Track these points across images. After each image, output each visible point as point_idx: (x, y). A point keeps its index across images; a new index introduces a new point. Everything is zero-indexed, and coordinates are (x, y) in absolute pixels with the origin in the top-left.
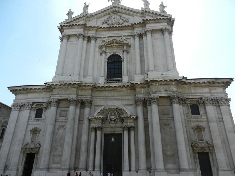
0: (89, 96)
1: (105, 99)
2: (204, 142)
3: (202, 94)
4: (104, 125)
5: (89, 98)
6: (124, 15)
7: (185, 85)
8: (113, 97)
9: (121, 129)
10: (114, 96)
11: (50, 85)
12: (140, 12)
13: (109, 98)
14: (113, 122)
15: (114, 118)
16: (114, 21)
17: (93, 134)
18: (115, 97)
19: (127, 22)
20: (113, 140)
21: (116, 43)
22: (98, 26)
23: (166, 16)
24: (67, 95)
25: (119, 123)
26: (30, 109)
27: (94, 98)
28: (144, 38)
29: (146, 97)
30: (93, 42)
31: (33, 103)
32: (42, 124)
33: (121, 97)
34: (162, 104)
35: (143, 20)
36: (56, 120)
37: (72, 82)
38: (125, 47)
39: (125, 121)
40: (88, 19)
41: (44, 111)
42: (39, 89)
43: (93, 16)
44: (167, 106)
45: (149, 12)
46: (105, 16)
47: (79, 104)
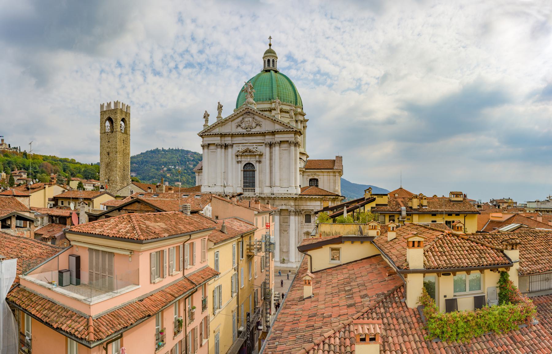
6: (256, 117)
19: (259, 125)
23: (292, 128)
46: (238, 117)
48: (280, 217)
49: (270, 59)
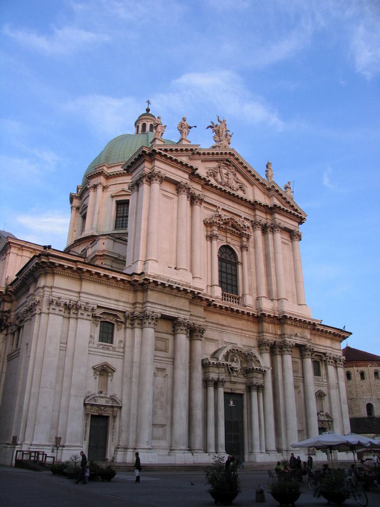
1: (219, 329)
2: (324, 414)
3: (325, 348)
10: (232, 327)
12: (265, 185)
13: (224, 328)
14: (235, 374)
17: (211, 390)
18: (233, 330)
20: (231, 403)
21: (233, 226)
23: (300, 213)
24: (175, 310)
25: (241, 376)
28: (270, 236)
29: (279, 340)
32: (115, 356)
37: (182, 285)
38: (245, 239)
41: (118, 330)
43: (199, 154)
44: (296, 359)
49: (146, 122)
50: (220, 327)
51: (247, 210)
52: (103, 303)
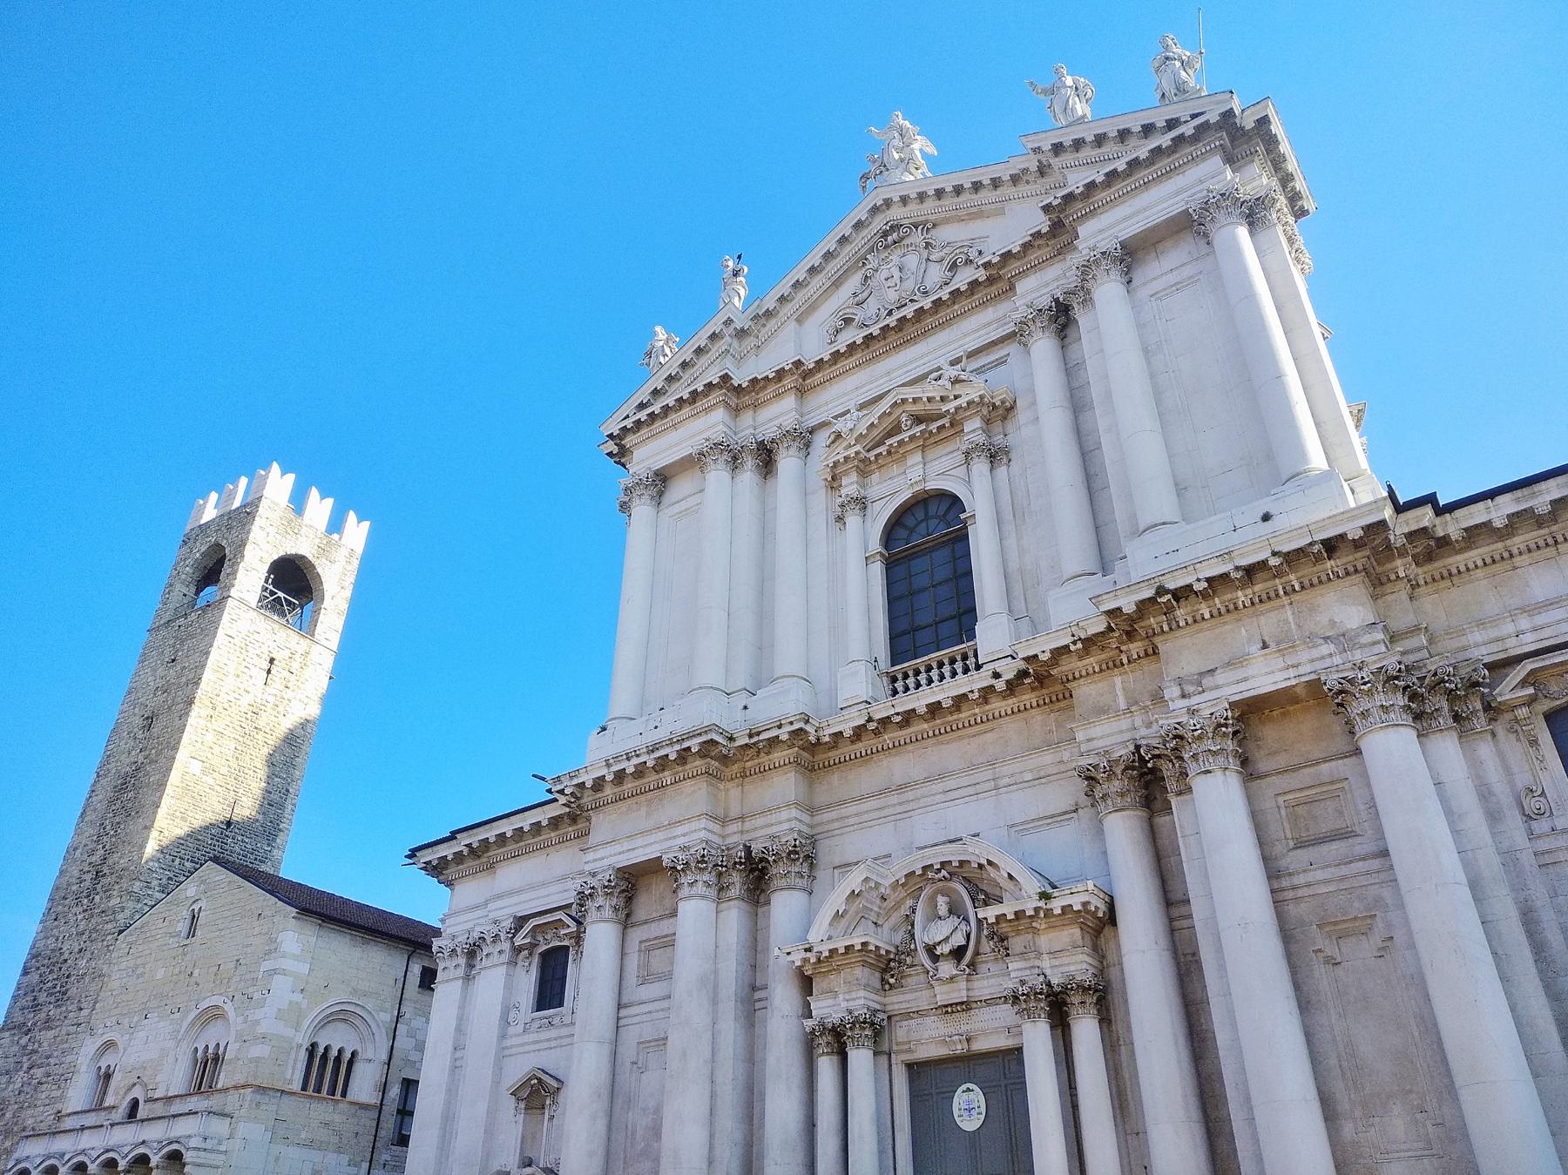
0: (785, 815)
1: (890, 811)
4: (897, 1001)
5: (786, 826)
7: (1457, 561)
8: (938, 787)
9: (1005, 1014)
10: (941, 777)
11: (567, 791)
13: (910, 795)
14: (947, 968)
15: (946, 939)
16: (892, 296)
17: (826, 1067)
18: (951, 784)
21: (918, 420)
22: (798, 364)
23: (1194, 116)
24: (661, 835)
26: (505, 957)
27: (826, 816)
30: (787, 462)
31: (521, 921)
33: (989, 775)
34: (1281, 761)
35: (1047, 209)
36: (620, 1007)
39: (1016, 943)
40: (750, 342)
42: (537, 827)
44: (1325, 767)
45: (1078, 144)
46: (837, 283)
47: (736, 878)
48: (1250, 799)
50: (894, 799)
51: (990, 314)
52: (527, 906)
